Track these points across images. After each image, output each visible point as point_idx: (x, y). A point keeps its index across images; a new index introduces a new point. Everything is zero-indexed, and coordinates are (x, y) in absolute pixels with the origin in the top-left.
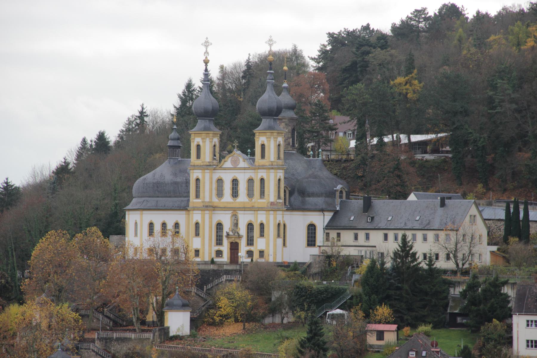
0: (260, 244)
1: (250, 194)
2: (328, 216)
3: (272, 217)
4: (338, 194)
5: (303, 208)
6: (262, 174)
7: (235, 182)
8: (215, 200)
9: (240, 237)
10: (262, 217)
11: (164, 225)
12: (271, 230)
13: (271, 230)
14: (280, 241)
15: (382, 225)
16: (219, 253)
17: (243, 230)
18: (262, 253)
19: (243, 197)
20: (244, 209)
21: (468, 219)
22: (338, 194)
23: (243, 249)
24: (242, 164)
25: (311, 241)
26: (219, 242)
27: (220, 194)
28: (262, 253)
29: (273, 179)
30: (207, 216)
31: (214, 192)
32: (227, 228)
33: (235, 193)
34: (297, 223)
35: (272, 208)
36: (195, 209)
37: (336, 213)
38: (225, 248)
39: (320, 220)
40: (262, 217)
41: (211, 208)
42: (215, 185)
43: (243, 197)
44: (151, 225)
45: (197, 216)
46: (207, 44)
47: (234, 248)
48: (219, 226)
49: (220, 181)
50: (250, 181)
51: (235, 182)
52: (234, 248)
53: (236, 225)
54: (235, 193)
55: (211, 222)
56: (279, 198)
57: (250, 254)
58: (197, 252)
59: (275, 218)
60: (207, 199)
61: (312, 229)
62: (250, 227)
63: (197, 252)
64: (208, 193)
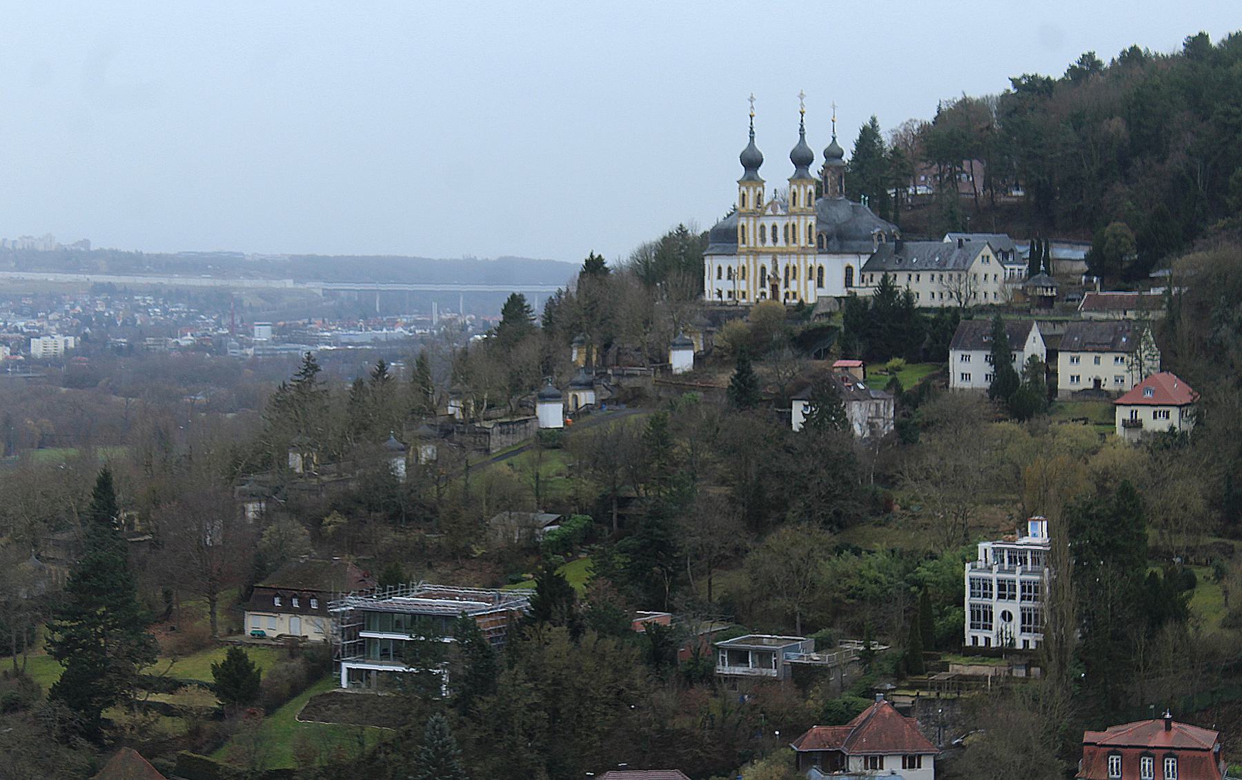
0: (793, 286)
1: (787, 241)
2: (864, 260)
3: (802, 261)
4: (875, 238)
5: (840, 251)
6: (794, 220)
7: (774, 228)
8: (759, 245)
9: (779, 280)
10: (793, 261)
11: (730, 269)
12: (802, 273)
13: (802, 273)
14: (812, 284)
15: (907, 267)
16: (763, 294)
17: (781, 275)
18: (794, 294)
19: (781, 243)
20: (782, 254)
21: (979, 257)
22: (875, 238)
23: (782, 291)
24: (780, 212)
25: (848, 282)
26: (763, 285)
27: (763, 240)
28: (794, 294)
29: (802, 224)
30: (751, 261)
31: (759, 238)
32: (769, 272)
33: (775, 240)
34: (834, 267)
35: (804, 252)
36: (743, 254)
37: (873, 255)
38: (768, 290)
39: (857, 263)
40: (793, 261)
41: (756, 253)
42: (758, 232)
43: (781, 243)
44: (720, 268)
45: (743, 261)
46: (752, 99)
47: (775, 288)
48: (763, 269)
49: (763, 227)
50: (786, 227)
51: (774, 228)
52: (775, 288)
53: (776, 268)
54: (775, 240)
55: (755, 267)
56: (811, 242)
57: (787, 295)
58: (744, 293)
59: (805, 262)
60: (752, 245)
61: (849, 270)
62: (787, 268)
63: (744, 293)
64: (752, 240)
